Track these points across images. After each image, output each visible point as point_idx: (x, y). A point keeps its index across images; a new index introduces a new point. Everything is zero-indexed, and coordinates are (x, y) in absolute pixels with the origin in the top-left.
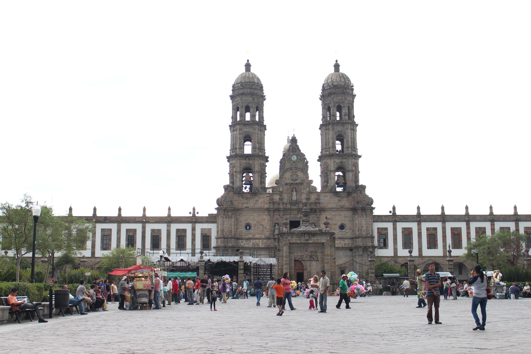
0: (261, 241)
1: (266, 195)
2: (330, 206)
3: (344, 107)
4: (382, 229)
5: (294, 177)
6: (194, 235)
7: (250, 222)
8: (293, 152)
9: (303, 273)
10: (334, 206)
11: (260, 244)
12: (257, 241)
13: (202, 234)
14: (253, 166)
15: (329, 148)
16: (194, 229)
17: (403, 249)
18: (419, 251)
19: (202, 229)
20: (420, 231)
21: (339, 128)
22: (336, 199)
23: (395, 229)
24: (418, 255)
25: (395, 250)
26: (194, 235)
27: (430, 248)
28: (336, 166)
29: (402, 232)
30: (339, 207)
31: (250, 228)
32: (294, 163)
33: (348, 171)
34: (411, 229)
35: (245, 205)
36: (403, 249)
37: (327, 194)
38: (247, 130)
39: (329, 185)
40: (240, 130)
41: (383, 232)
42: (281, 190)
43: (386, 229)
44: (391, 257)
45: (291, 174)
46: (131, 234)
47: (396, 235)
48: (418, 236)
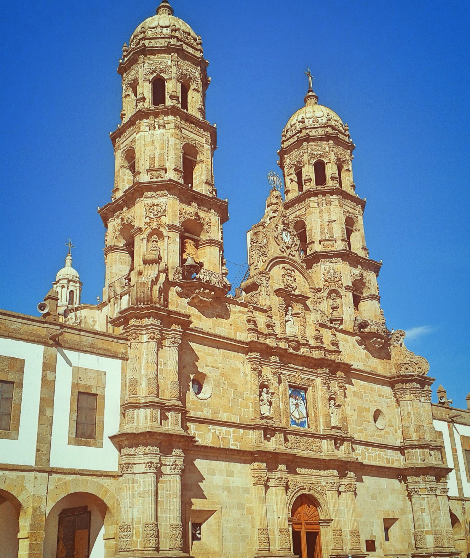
0: (232, 430)
9: (318, 532)
11: (232, 442)
12: (224, 429)
13: (74, 386)
14: (206, 227)
16: (49, 366)
19: (77, 371)
22: (362, 351)
26: (48, 385)
32: (288, 248)
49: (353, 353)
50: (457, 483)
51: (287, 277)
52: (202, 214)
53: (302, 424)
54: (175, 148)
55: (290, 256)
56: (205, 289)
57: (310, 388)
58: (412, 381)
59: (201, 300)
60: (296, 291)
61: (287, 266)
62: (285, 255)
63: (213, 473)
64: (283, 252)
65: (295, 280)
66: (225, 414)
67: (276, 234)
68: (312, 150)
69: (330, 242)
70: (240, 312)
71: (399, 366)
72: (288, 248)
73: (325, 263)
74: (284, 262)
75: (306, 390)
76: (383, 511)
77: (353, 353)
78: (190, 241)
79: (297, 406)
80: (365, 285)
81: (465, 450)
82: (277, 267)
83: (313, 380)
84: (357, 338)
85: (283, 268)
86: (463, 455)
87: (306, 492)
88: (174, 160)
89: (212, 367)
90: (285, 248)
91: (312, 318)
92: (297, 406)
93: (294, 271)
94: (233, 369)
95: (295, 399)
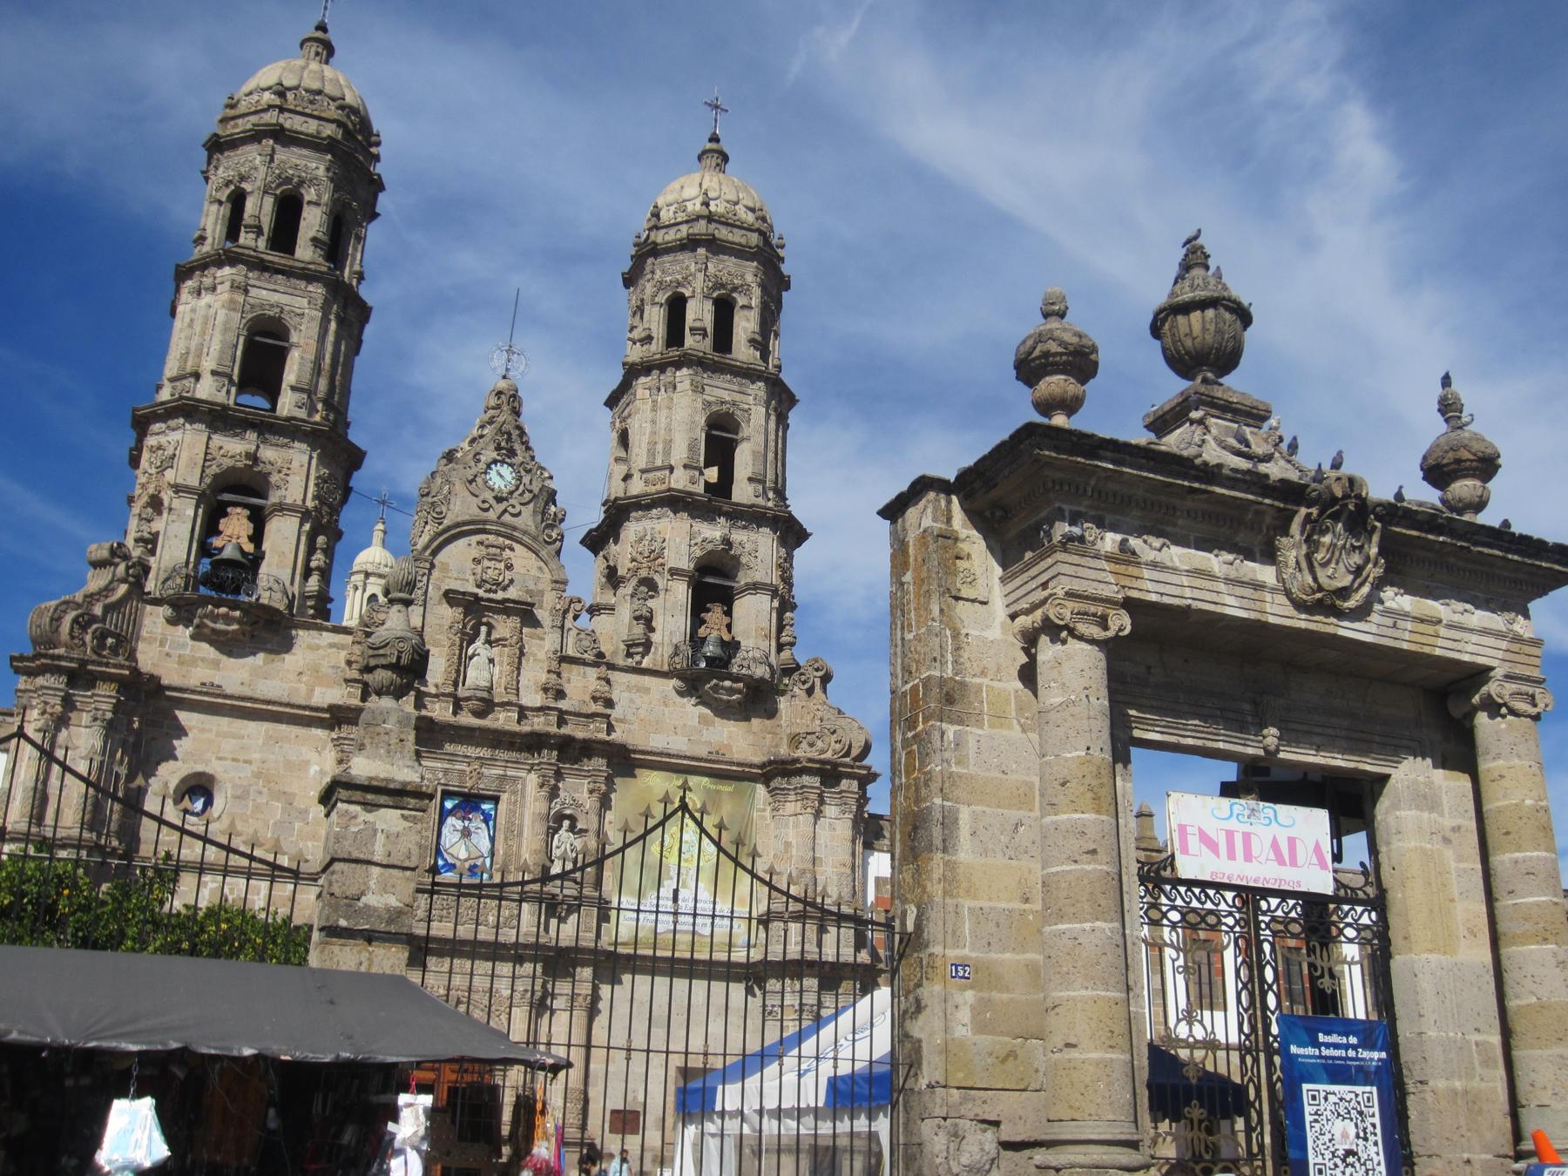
1: (328, 637)
2: (657, 742)
3: (749, 307)
5: (493, 570)
7: (212, 767)
8: (499, 448)
10: (678, 744)
14: (274, 478)
15: (671, 469)
21: (722, 390)
22: (691, 711)
28: (699, 553)
30: (702, 752)
31: (209, 803)
32: (499, 499)
33: (755, 587)
37: (647, 680)
38: (275, 298)
39: (656, 637)
40: (234, 287)
45: (476, 552)
49: (656, 714)
51: (486, 563)
52: (267, 453)
54: (226, 330)
55: (507, 518)
56: (218, 607)
57: (504, 797)
58: (801, 772)
59: (213, 630)
60: (511, 589)
62: (492, 515)
64: (486, 510)
65: (509, 567)
67: (469, 474)
68: (663, 272)
69: (658, 474)
70: (332, 645)
71: (795, 740)
72: (499, 499)
73: (638, 520)
75: (496, 800)
77: (656, 714)
78: (239, 510)
79: (466, 833)
80: (739, 563)
82: (462, 542)
83: (515, 779)
84: (675, 682)
85: (480, 543)
88: (222, 351)
89: (234, 760)
90: (493, 502)
91: (541, 646)
92: (466, 833)
93: (512, 549)
94: (289, 765)
95: (463, 819)
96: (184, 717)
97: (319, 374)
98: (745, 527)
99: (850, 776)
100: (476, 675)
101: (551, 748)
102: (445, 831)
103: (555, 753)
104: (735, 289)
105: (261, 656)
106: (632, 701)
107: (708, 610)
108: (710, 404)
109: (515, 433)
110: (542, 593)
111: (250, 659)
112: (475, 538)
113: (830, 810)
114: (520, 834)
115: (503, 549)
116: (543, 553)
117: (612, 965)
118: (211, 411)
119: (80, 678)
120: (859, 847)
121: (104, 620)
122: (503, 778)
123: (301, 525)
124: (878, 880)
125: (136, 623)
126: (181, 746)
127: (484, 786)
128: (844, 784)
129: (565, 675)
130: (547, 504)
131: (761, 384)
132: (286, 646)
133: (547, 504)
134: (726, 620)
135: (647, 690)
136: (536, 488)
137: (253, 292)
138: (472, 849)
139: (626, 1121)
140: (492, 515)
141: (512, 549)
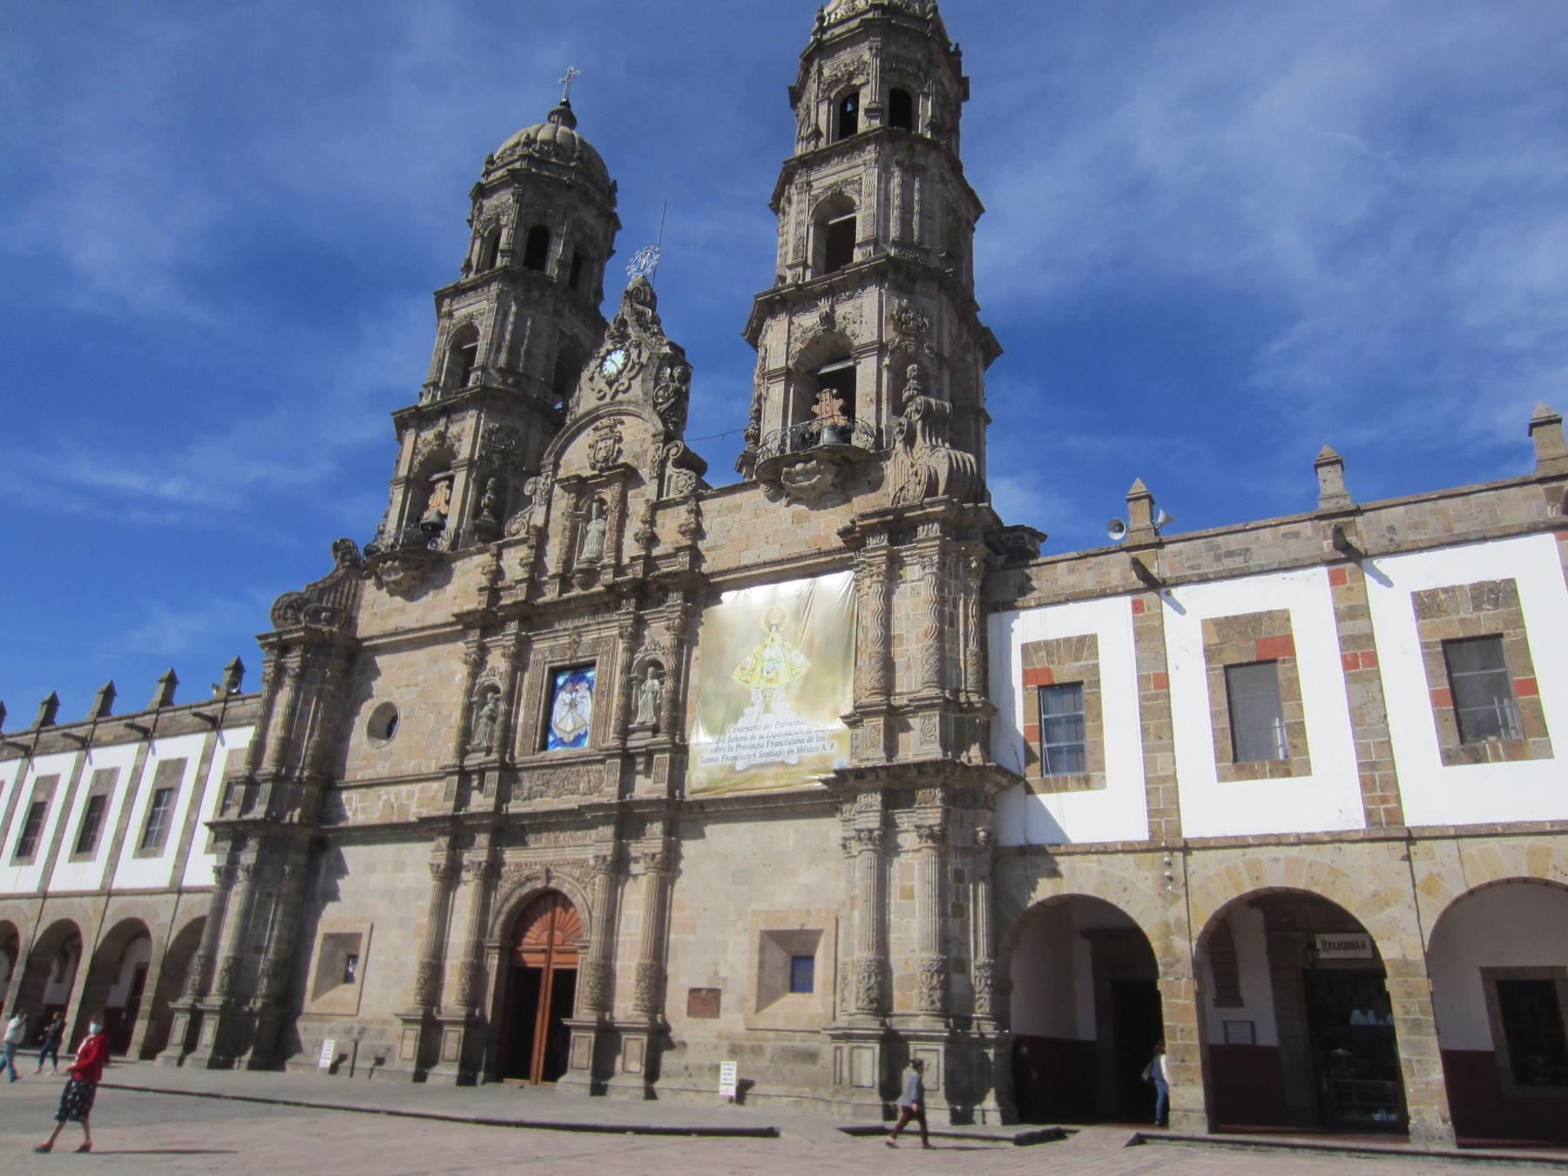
4: (1049, 647)
6: (201, 782)
12: (404, 788)
17: (1222, 777)
18: (1366, 785)
20: (1357, 627)
22: (783, 512)
23: (1149, 637)
24: (1355, 820)
25: (1162, 792)
26: (201, 782)
27: (1477, 758)
29: (1210, 654)
34: (1283, 617)
35: (392, 624)
36: (1222, 777)
41: (1064, 672)
42: (538, 520)
43: (1085, 645)
44: (1128, 849)
46: (41, 797)
47: (1162, 681)
48: (1349, 663)
50: (1148, 792)
53: (577, 740)
57: (598, 658)
59: (394, 582)
61: (605, 422)
63: (370, 869)
65: (620, 440)
66: (412, 763)
74: (598, 418)
76: (767, 912)
81: (1227, 668)
85: (596, 429)
86: (1210, 686)
87: (539, 885)
90: (606, 388)
92: (573, 705)
93: (622, 423)
96: (381, 661)
97: (499, 350)
98: (850, 297)
99: (928, 519)
100: (589, 550)
101: (627, 597)
102: (557, 707)
103: (633, 601)
104: (851, 75)
105: (431, 593)
106: (723, 524)
107: (817, 402)
108: (816, 197)
109: (630, 320)
110: (645, 452)
111: (424, 599)
112: (589, 430)
113: (912, 572)
114: (610, 692)
115: (612, 428)
116: (646, 415)
117: (685, 815)
118: (411, 415)
119: (284, 648)
120: (966, 611)
121: (320, 600)
122: (597, 642)
123: (469, 476)
124: (1025, 648)
125: (355, 596)
126: (377, 685)
127: (583, 656)
128: (922, 532)
129: (659, 522)
130: (660, 369)
131: (871, 148)
132: (447, 578)
133: (660, 369)
134: (840, 402)
135: (739, 507)
136: (644, 359)
137: (456, 314)
138: (578, 719)
139: (705, 1001)
140: (607, 400)
141: (622, 423)
